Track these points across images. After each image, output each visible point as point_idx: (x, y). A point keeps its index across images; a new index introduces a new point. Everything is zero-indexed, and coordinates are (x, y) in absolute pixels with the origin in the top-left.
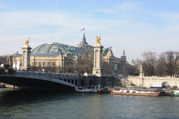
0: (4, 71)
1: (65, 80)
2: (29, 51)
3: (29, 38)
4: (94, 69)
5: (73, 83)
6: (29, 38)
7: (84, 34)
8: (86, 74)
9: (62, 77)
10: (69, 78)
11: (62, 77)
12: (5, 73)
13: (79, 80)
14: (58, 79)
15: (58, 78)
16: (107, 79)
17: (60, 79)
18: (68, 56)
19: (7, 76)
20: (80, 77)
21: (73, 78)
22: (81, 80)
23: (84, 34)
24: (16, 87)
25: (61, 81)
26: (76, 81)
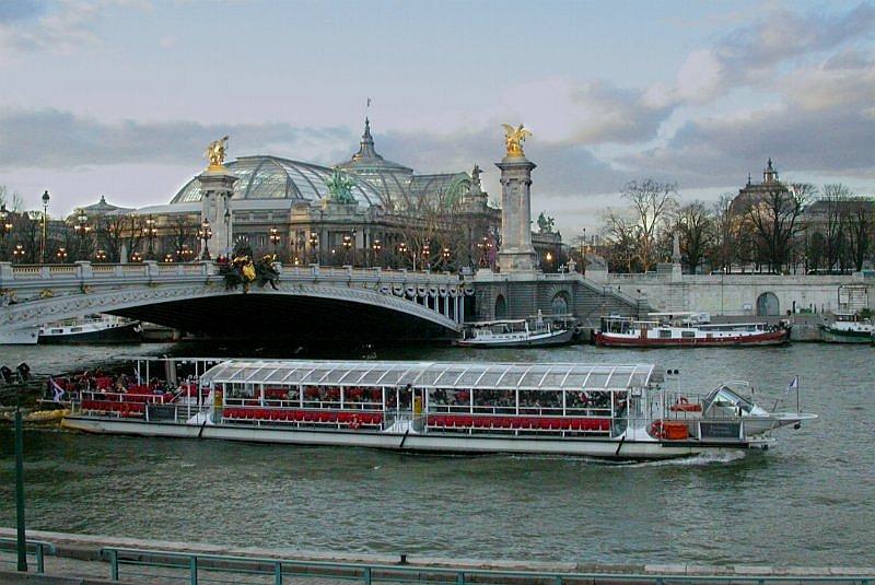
0: (242, 273)
1: (420, 301)
2: (230, 190)
3: (226, 139)
4: (506, 251)
5: (442, 311)
6: (226, 139)
7: (367, 123)
8: (484, 275)
9: (411, 290)
10: (433, 291)
11: (411, 290)
12: (246, 281)
13: (459, 297)
14: (401, 296)
15: (400, 292)
16: (554, 290)
17: (409, 298)
18: (334, 208)
19: (249, 292)
20: (461, 286)
21: (443, 291)
22: (466, 297)
23: (367, 123)
24: (190, 336)
25: (407, 303)
26: (451, 300)
